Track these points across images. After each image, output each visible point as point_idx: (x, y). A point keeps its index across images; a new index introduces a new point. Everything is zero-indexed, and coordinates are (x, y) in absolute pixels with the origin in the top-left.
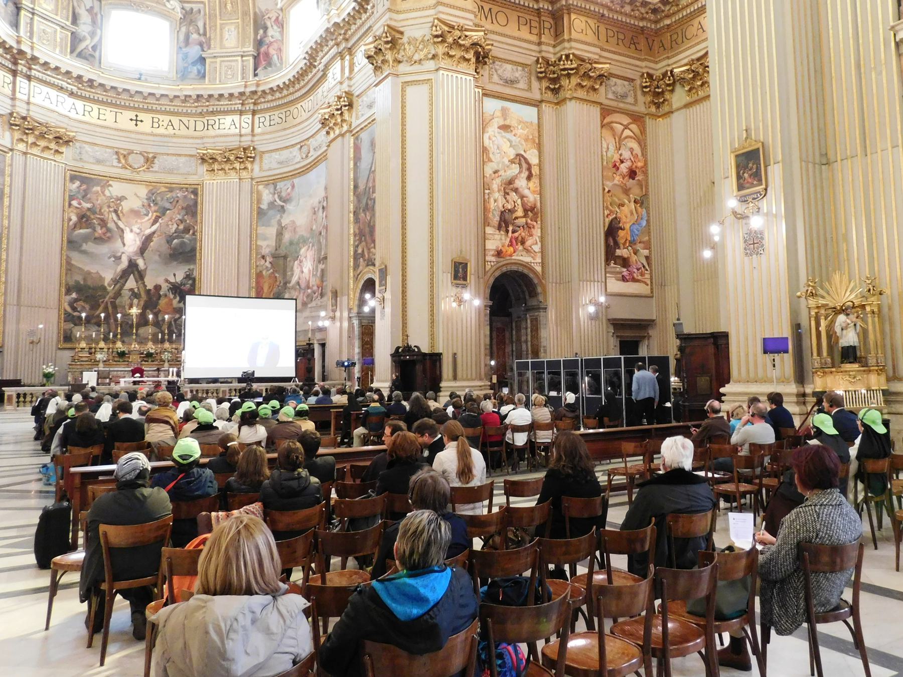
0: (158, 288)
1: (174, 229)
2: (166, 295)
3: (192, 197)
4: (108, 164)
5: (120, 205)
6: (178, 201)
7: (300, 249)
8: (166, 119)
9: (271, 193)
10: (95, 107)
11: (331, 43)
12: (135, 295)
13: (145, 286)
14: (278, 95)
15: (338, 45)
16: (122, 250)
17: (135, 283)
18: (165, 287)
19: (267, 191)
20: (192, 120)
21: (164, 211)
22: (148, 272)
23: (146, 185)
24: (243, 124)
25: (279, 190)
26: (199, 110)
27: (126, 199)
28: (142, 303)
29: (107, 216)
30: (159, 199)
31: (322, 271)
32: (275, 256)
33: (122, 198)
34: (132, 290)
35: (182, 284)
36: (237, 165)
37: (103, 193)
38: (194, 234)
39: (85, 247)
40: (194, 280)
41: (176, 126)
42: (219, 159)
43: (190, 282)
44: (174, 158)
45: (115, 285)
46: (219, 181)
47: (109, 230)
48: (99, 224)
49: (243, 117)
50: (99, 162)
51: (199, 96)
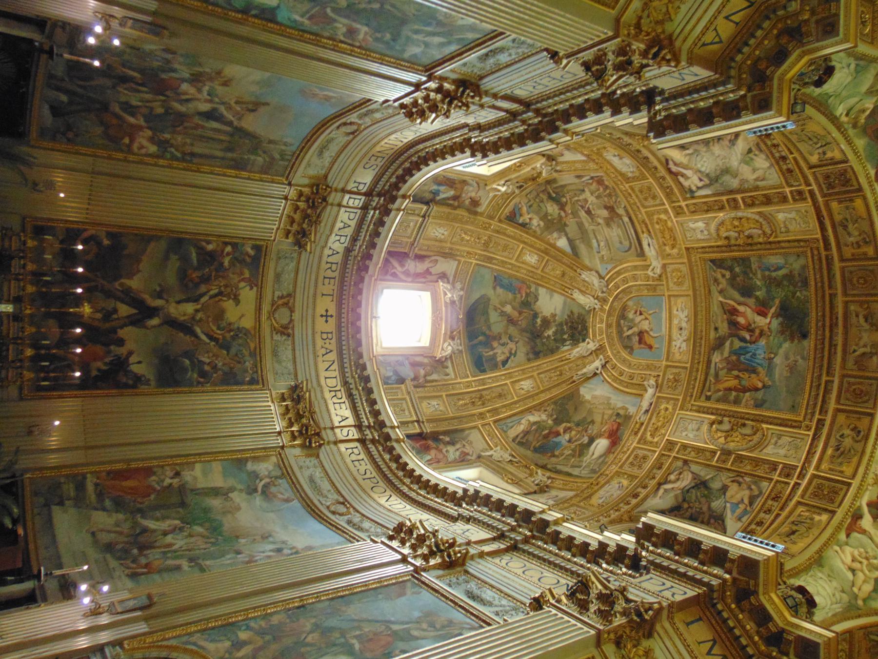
0: (121, 342)
1: (203, 359)
2: (109, 352)
3: (247, 379)
4: (276, 286)
5: (229, 298)
6: (239, 362)
7: (201, 525)
8: (333, 345)
9: (270, 472)
10: (336, 274)
11: (510, 520)
12: (108, 315)
13: (121, 328)
14: (394, 466)
15: (513, 529)
16: (171, 300)
17: (125, 314)
18: (123, 351)
19: (271, 468)
20: (337, 373)
21: (225, 346)
22: (143, 331)
23: (255, 328)
24: (345, 430)
25: (276, 483)
26: (350, 380)
27: (237, 305)
28: (96, 324)
29: (215, 283)
30: (240, 341)
31: (178, 568)
32: (182, 490)
33: (237, 301)
34: (115, 311)
35: (127, 372)
36: (295, 428)
37: (243, 280)
38: (199, 383)
39: (174, 258)
40: (134, 387)
41: (327, 357)
42: (301, 406)
43: (131, 382)
44: (290, 357)
45: (122, 291)
46: (272, 408)
47: (197, 285)
48: (204, 275)
49: (353, 429)
50: (278, 277)
51: (367, 379)
